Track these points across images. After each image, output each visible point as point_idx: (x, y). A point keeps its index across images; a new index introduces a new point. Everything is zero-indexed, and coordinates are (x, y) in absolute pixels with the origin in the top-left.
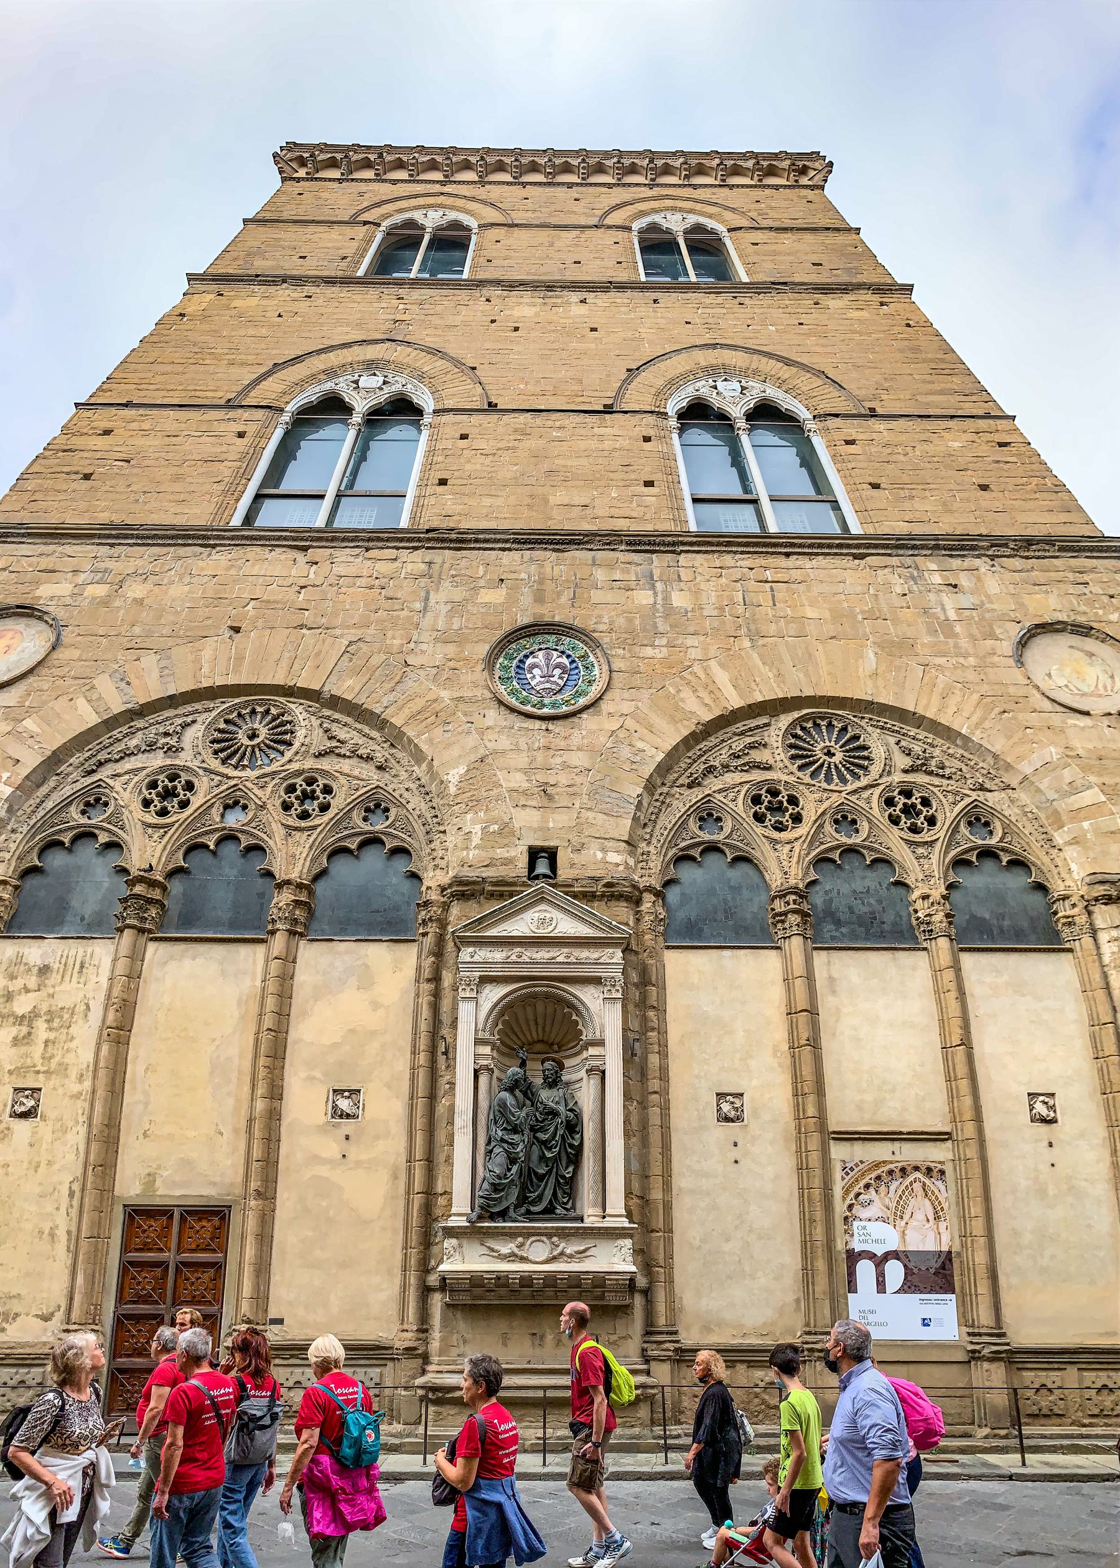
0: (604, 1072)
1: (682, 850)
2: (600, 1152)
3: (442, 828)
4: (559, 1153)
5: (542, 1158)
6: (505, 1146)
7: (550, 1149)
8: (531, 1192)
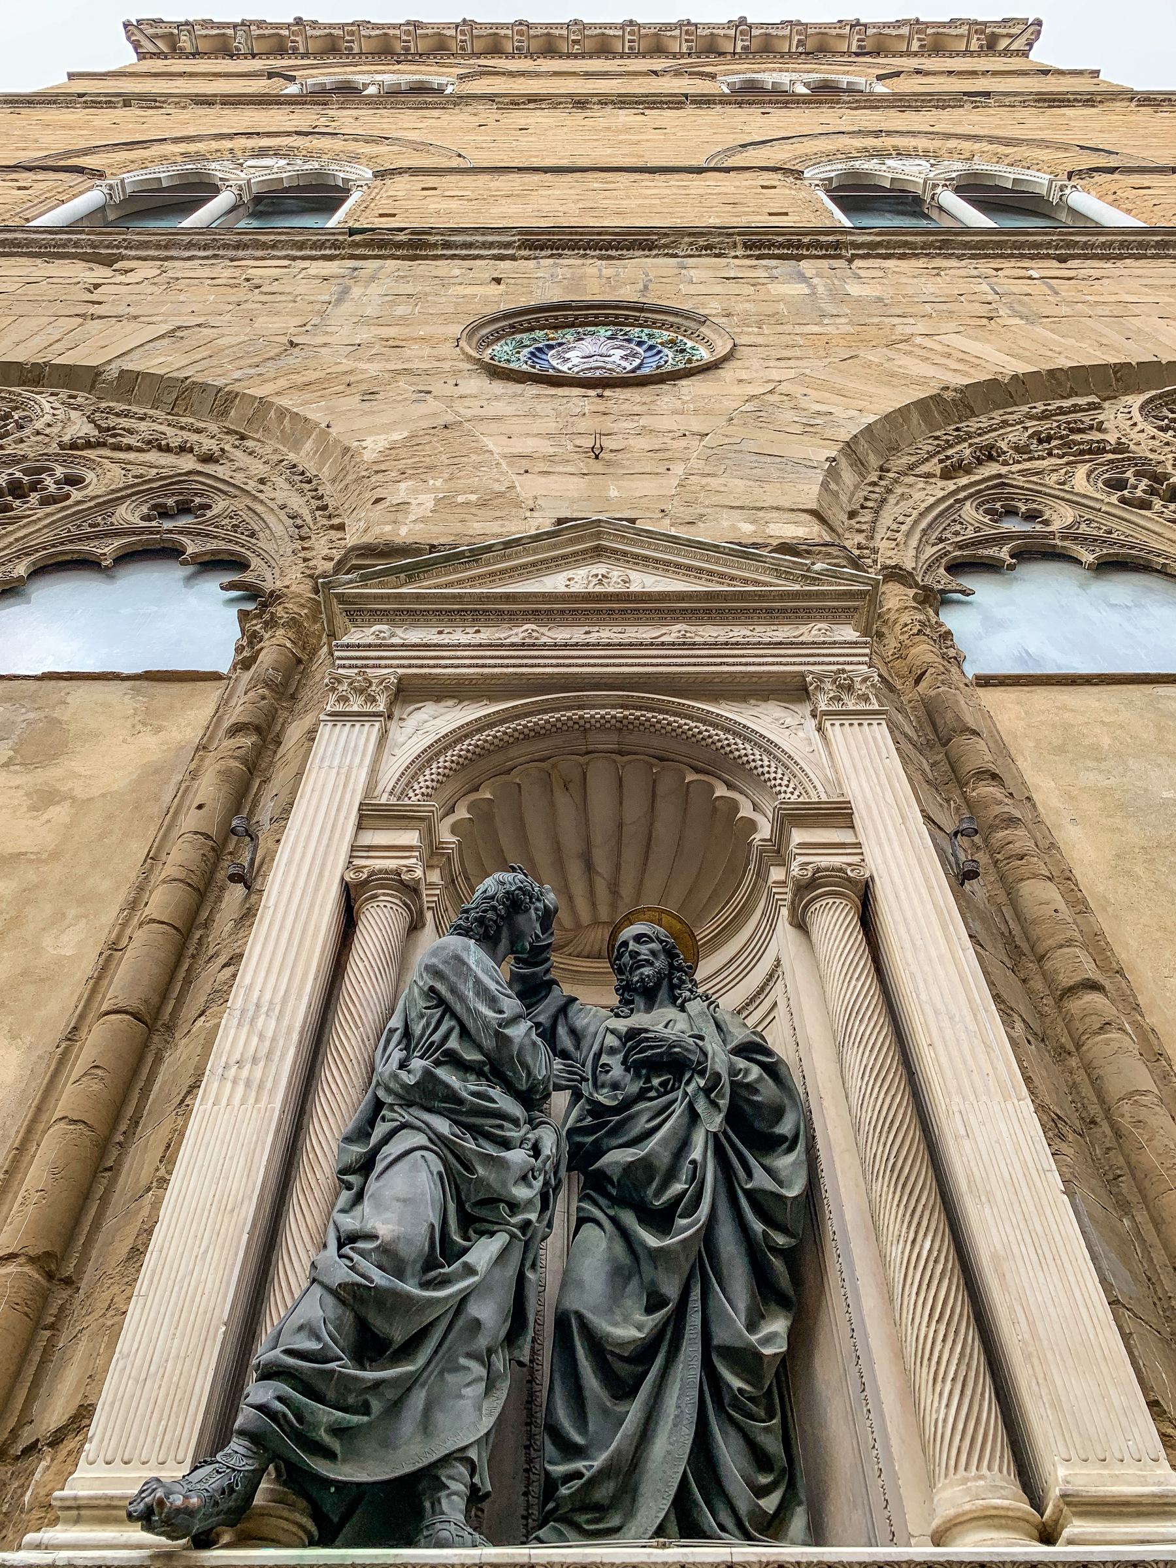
0: (865, 904)
1: (960, 546)
2: (923, 1173)
3: (336, 521)
4: (709, 1232)
5: (632, 1264)
6: (442, 1125)
7: (661, 1221)
8: (571, 1451)
